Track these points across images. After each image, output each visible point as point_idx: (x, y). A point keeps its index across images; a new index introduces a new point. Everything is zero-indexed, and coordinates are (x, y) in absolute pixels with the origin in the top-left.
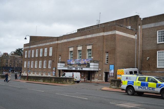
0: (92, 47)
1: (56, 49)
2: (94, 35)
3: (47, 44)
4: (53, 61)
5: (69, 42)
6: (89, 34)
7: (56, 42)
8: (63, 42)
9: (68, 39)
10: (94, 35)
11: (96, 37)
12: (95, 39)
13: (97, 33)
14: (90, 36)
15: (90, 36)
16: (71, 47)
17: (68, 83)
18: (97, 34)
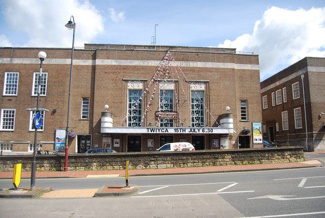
0: (206, 88)
1: (68, 79)
2: (209, 65)
3: (17, 61)
4: (54, 112)
5: (125, 68)
6: (195, 61)
7: (68, 61)
8: (102, 66)
9: (123, 61)
10: (209, 65)
11: (217, 70)
12: (213, 73)
13: (219, 61)
14: (200, 65)
15: (200, 65)
16: (133, 81)
17: (293, 159)
18: (219, 63)
